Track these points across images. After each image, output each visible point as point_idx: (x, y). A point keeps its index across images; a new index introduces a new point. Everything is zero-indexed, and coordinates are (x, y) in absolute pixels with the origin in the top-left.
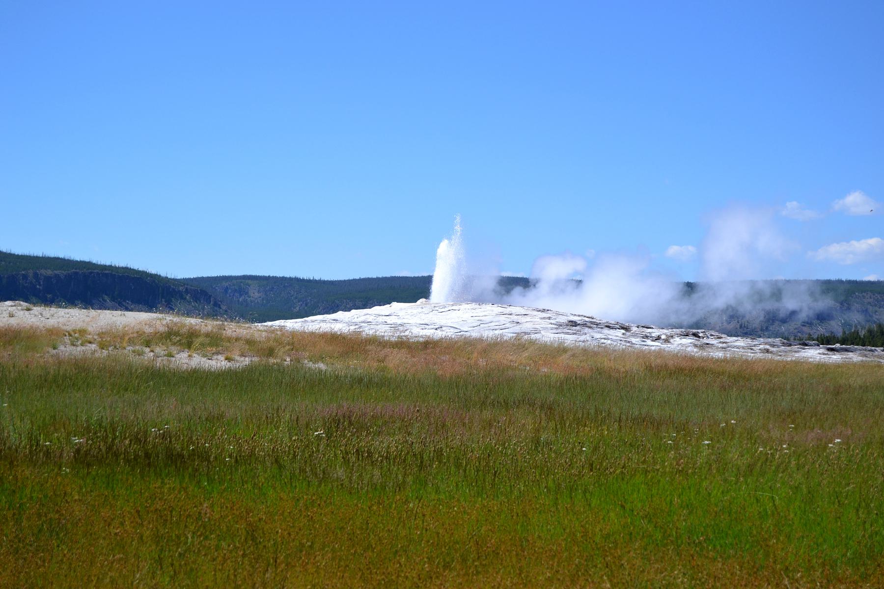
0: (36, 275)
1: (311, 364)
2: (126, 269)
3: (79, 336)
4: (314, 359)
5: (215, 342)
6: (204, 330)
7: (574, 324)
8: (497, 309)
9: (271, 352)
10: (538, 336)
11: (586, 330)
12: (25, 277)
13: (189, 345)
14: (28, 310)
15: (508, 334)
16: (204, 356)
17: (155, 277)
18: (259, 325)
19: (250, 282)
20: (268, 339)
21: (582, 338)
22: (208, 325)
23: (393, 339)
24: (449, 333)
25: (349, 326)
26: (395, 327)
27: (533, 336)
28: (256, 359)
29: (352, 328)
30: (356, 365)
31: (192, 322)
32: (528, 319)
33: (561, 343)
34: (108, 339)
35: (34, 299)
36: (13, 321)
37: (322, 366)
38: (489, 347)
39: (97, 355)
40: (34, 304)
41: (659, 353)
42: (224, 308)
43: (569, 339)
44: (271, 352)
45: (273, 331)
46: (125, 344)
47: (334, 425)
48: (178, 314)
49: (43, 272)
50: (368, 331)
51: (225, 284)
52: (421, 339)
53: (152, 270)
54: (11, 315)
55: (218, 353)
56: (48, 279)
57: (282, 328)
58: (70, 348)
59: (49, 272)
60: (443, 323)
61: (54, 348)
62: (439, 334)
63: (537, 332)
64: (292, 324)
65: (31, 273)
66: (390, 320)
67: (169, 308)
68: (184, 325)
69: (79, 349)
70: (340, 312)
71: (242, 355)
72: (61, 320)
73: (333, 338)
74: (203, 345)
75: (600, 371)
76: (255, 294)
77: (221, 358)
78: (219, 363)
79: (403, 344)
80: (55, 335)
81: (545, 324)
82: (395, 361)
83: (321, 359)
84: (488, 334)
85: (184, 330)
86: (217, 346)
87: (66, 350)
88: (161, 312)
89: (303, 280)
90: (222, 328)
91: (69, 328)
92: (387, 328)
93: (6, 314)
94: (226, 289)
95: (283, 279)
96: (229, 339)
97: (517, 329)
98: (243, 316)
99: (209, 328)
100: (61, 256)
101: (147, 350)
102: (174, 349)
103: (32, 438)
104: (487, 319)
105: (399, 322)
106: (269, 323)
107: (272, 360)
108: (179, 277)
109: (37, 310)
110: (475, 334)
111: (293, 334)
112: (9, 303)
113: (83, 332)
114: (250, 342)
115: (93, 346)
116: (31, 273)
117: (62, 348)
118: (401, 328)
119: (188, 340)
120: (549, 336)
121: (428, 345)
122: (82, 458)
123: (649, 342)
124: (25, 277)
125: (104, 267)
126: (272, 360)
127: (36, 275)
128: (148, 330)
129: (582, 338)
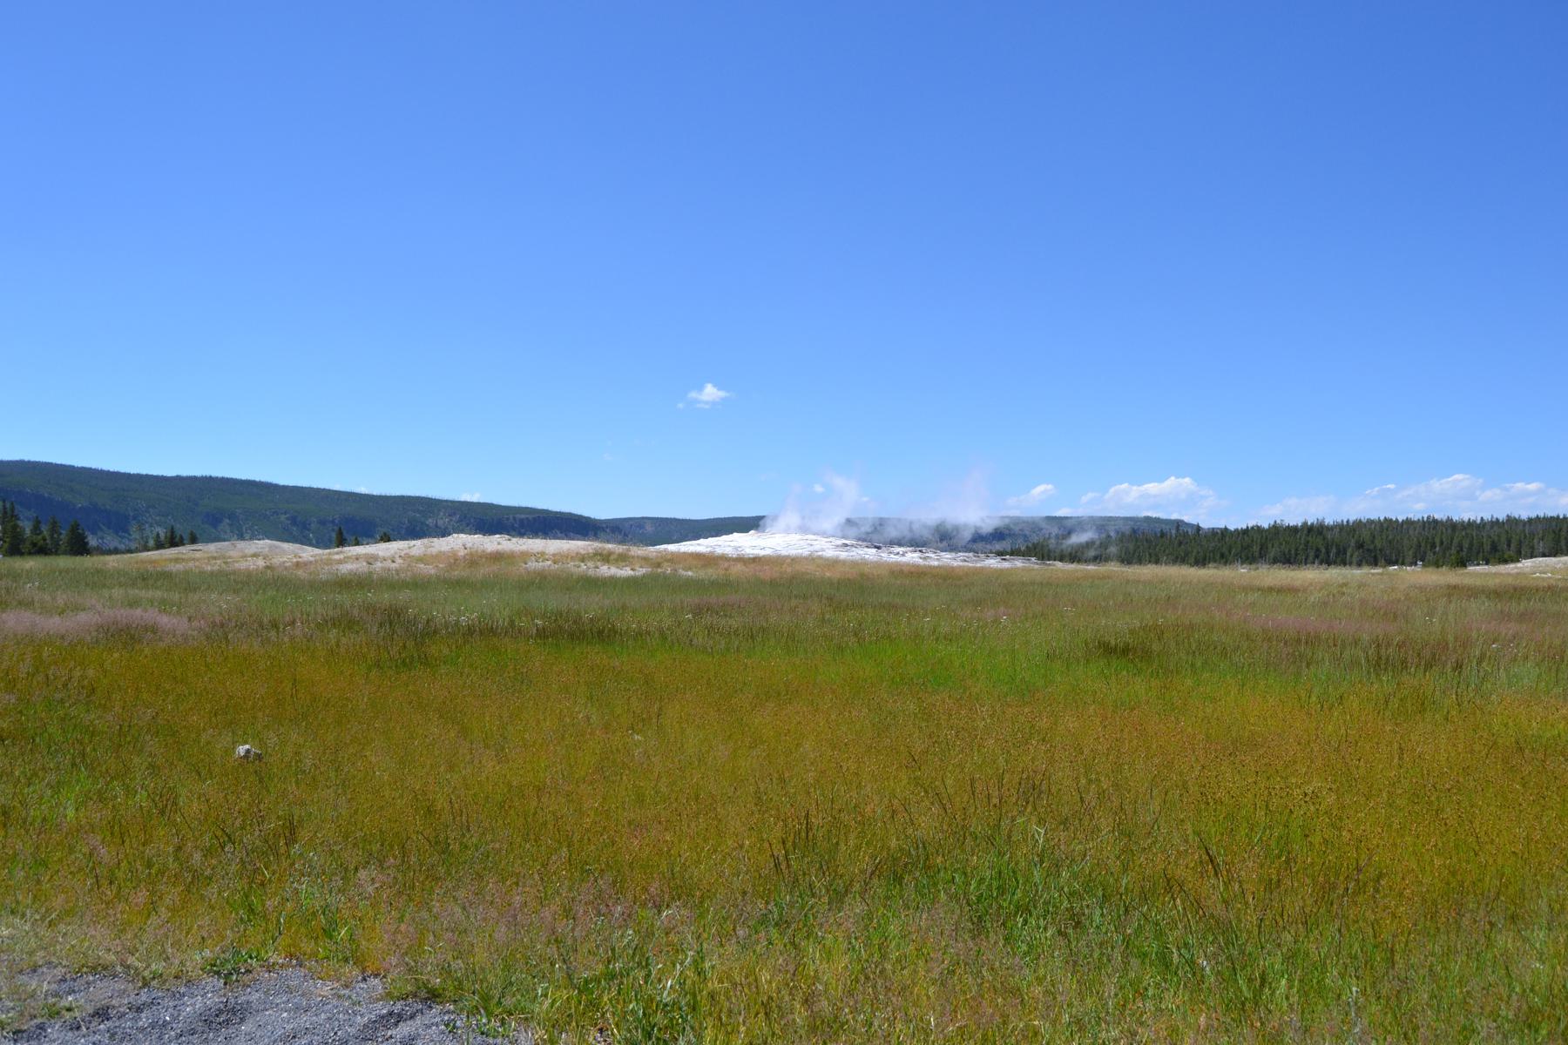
0: (514, 518)
1: (684, 573)
2: (570, 513)
3: (541, 556)
4: (685, 569)
5: (623, 559)
6: (617, 552)
7: (846, 545)
8: (798, 537)
9: (659, 565)
10: (824, 553)
11: (854, 549)
12: (508, 519)
13: (608, 562)
14: (509, 540)
15: (805, 553)
16: (618, 567)
17: (588, 519)
18: (651, 549)
19: (646, 521)
20: (657, 557)
21: (852, 554)
22: (617, 548)
23: (734, 556)
24: (768, 552)
25: (707, 548)
26: (736, 548)
27: (820, 553)
28: (650, 569)
29: (709, 549)
30: (711, 573)
31: (610, 546)
32: (817, 542)
33: (837, 557)
34: (558, 558)
35: (514, 533)
36: (500, 547)
37: (690, 573)
38: (794, 560)
39: (552, 568)
40: (513, 536)
41: (897, 564)
42: (630, 536)
43: (843, 555)
44: (659, 565)
45: (660, 552)
46: (569, 561)
47: (698, 611)
48: (601, 542)
49: (518, 516)
50: (719, 551)
51: (631, 522)
52: (751, 556)
53: (586, 514)
54: (499, 544)
55: (627, 566)
56: (522, 521)
57: (665, 550)
58: (535, 564)
59: (523, 516)
60: (763, 545)
61: (526, 564)
62: (762, 553)
63: (823, 550)
64: (672, 547)
65: (511, 516)
66: (732, 544)
67: (596, 537)
68: (605, 549)
69: (541, 564)
70: (702, 540)
71: (641, 567)
72: (531, 547)
73: (698, 556)
74: (617, 560)
75: (862, 575)
76: (649, 528)
77: (628, 569)
78: (626, 572)
79: (741, 560)
80: (525, 556)
81: (828, 545)
82: (738, 569)
83: (690, 569)
84: (793, 552)
85: (605, 552)
86: (625, 561)
87: (533, 565)
88: (592, 541)
89: (679, 520)
90: (629, 550)
91: (535, 551)
92: (730, 548)
93: (496, 543)
94: (631, 525)
95: (667, 519)
96: (633, 557)
97: (811, 549)
98: (642, 542)
99: (621, 550)
100: (530, 506)
101: (582, 564)
102: (599, 564)
103: (512, 622)
104: (792, 543)
105: (738, 545)
106: (658, 547)
107: (659, 570)
108: (603, 518)
109: (514, 540)
110: (784, 553)
111: (672, 553)
112: (498, 536)
113: (543, 554)
114: (645, 559)
115: (549, 563)
116: (511, 516)
117: (530, 563)
118: (740, 549)
119: (606, 558)
120: (830, 553)
121: (756, 560)
122: (542, 634)
123: (892, 556)
124: (508, 519)
125: (557, 513)
126: (659, 570)
127: (514, 518)
128: (583, 552)
129: (852, 554)
